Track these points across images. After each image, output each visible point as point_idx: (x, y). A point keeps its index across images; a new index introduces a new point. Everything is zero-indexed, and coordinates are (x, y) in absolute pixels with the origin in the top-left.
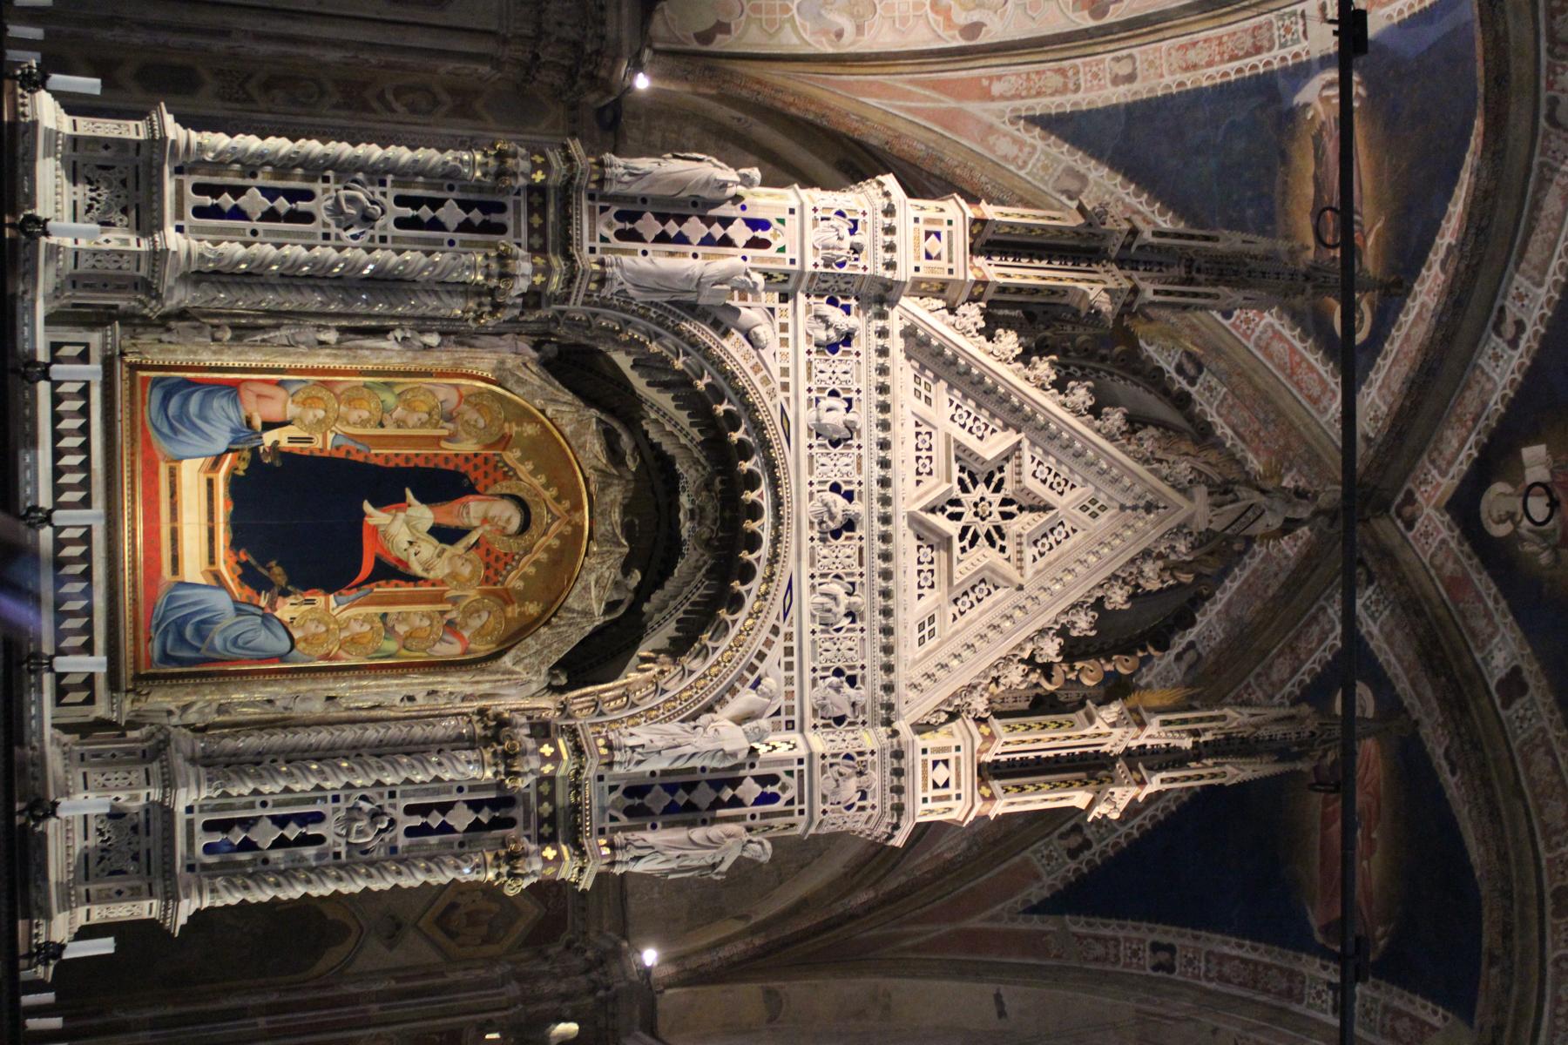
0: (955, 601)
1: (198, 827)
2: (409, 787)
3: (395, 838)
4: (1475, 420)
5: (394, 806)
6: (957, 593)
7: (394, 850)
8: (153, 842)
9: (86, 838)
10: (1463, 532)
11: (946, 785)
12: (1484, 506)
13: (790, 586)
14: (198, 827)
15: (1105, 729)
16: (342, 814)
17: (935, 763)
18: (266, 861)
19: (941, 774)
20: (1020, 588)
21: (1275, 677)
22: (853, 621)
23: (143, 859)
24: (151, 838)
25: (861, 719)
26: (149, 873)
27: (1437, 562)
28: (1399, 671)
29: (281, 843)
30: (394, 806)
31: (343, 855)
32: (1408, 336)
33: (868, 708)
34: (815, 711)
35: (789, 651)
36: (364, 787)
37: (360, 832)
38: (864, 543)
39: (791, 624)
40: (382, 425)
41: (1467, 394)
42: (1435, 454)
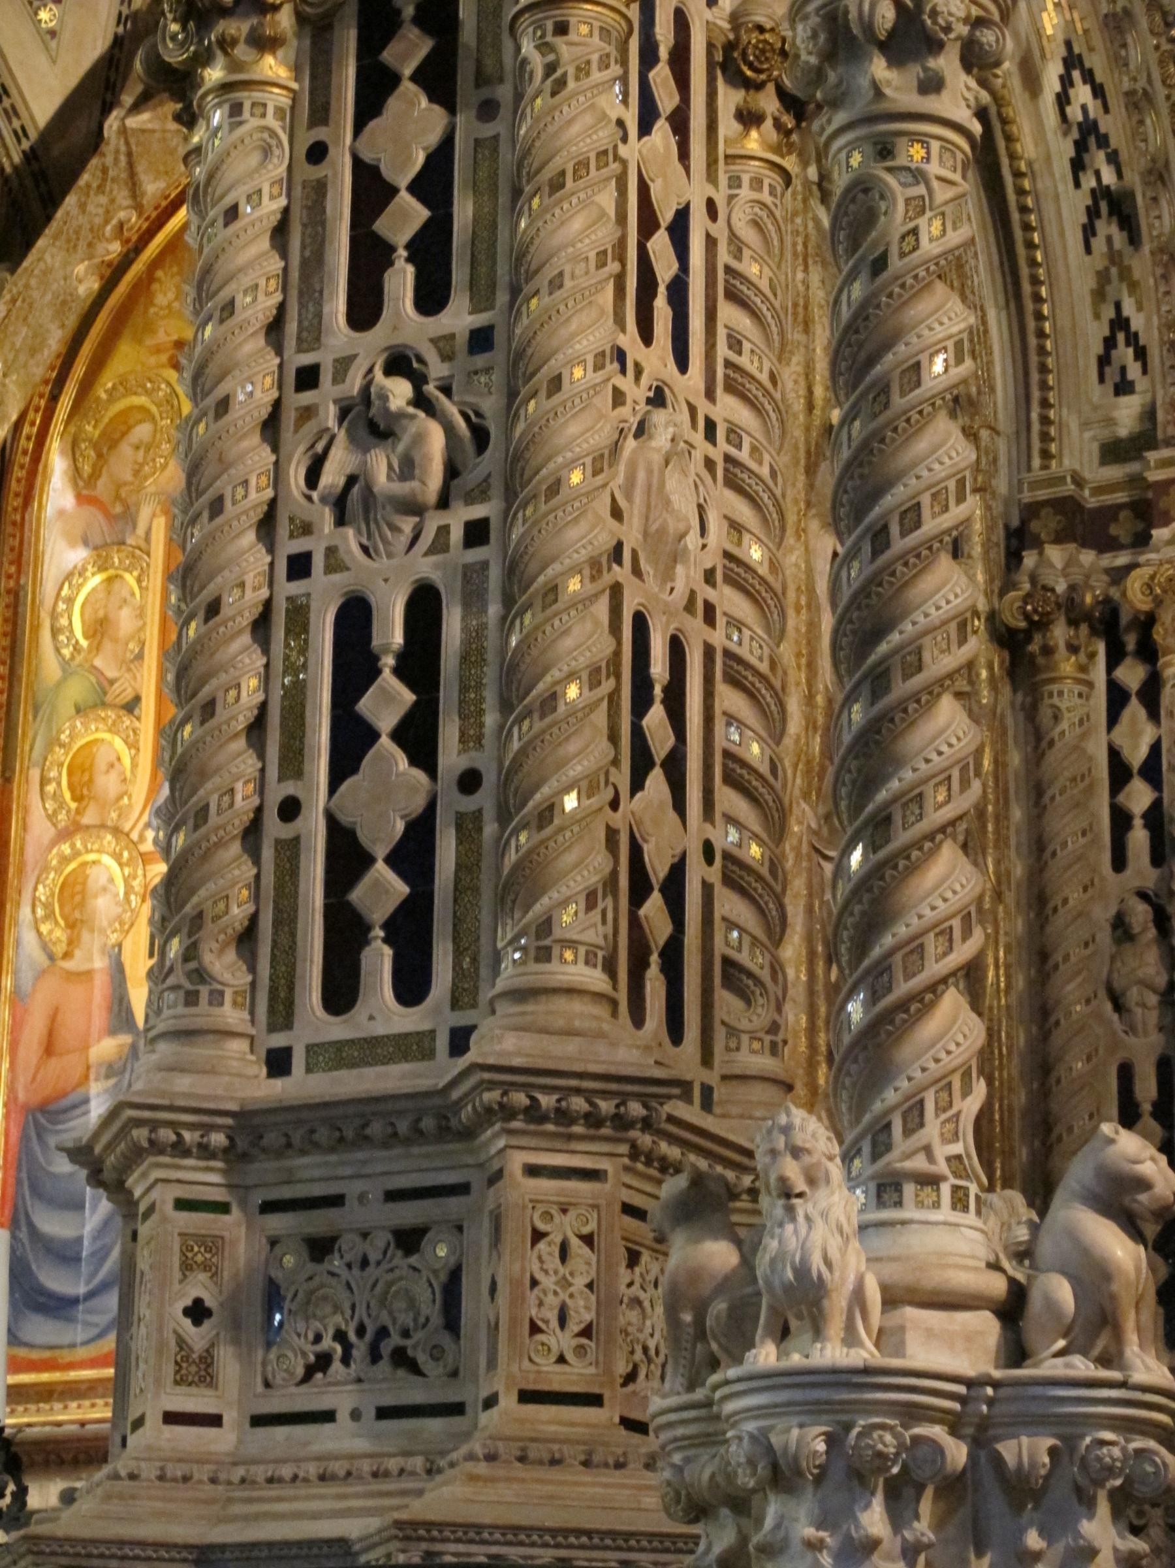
1: (337, 1029)
2: (291, 327)
3: (444, 345)
5: (343, 365)
7: (481, 340)
8: (364, 1184)
9: (328, 1416)
14: (337, 1029)
16: (350, 538)
18: (470, 781)
23: (409, 1214)
24: (352, 1189)
26: (462, 1189)
29: (418, 738)
30: (343, 365)
31: (478, 512)
36: (278, 475)
37: (407, 468)
40: (131, 706)
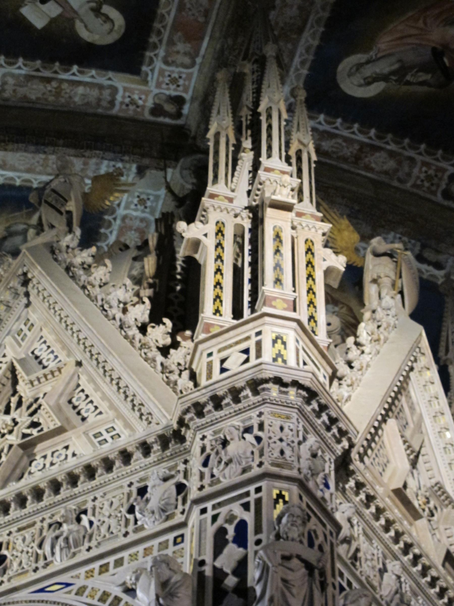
0: (84, 419)
4: (48, 80)
6: (77, 420)
10: (145, 49)
11: (246, 351)
12: (109, 40)
13: (42, 590)
15: (211, 228)
17: (223, 370)
19: (235, 362)
20: (79, 364)
21: (391, 164)
22: (85, 512)
25: (181, 467)
27: (187, 60)
28: (301, 49)
32: (28, 171)
33: (172, 463)
34: (168, 518)
35: (104, 569)
38: (14, 529)
39: (78, 577)
41: (33, 97)
42: (104, 104)
